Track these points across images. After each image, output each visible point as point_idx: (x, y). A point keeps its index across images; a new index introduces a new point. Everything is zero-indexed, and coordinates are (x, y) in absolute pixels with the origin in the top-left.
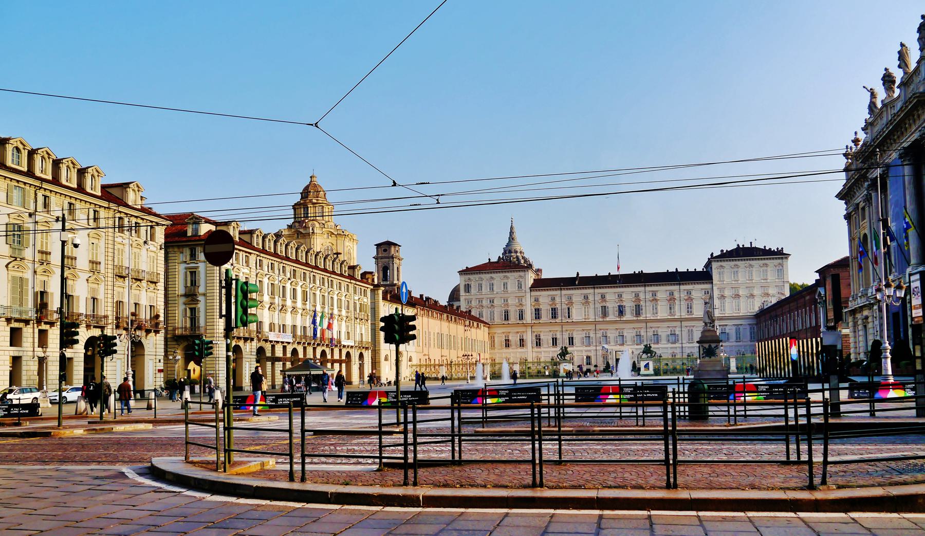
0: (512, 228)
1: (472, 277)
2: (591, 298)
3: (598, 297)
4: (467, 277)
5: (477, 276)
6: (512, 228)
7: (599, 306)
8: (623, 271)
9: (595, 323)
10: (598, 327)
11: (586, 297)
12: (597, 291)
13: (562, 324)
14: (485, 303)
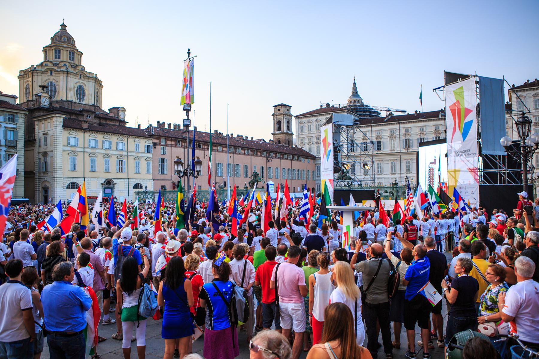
0: (355, 84)
1: (303, 120)
2: (397, 133)
3: (403, 132)
4: (300, 120)
5: (307, 119)
6: (355, 84)
7: (403, 138)
8: (425, 111)
9: (400, 154)
10: (403, 157)
11: (392, 132)
12: (402, 126)
13: (373, 155)
14: (314, 140)
